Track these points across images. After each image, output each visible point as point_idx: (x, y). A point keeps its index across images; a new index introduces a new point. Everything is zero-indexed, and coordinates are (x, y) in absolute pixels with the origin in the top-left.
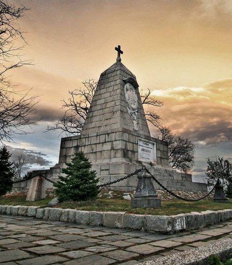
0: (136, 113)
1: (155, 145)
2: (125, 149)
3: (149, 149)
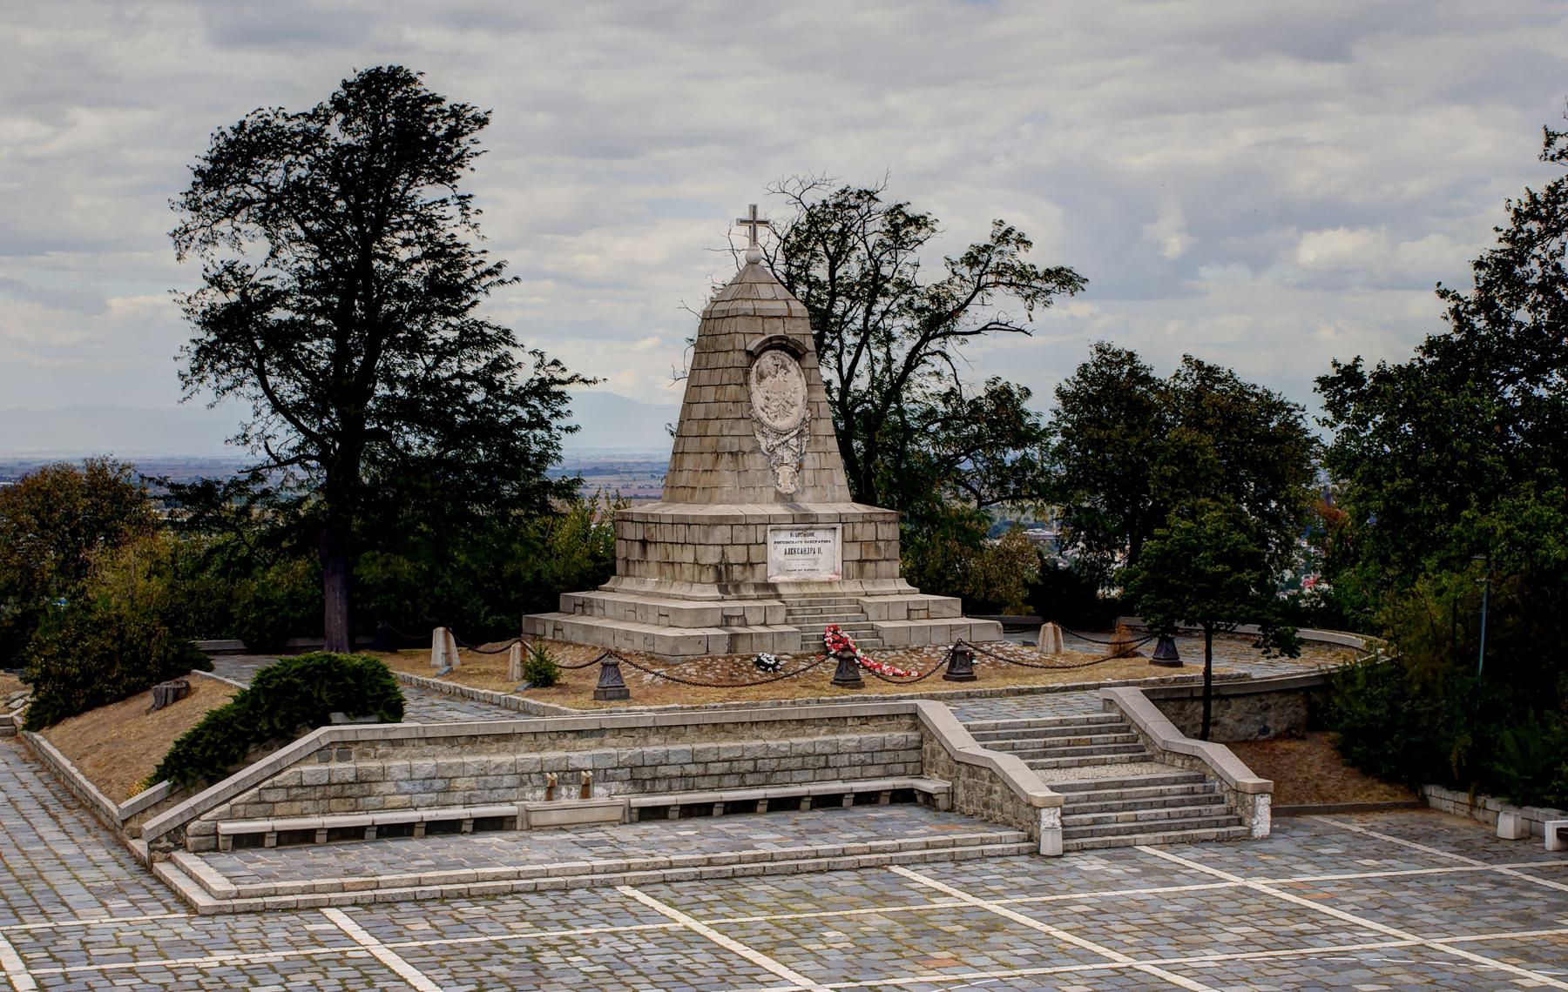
0: (794, 442)
1: (839, 532)
2: (721, 563)
3: (816, 546)
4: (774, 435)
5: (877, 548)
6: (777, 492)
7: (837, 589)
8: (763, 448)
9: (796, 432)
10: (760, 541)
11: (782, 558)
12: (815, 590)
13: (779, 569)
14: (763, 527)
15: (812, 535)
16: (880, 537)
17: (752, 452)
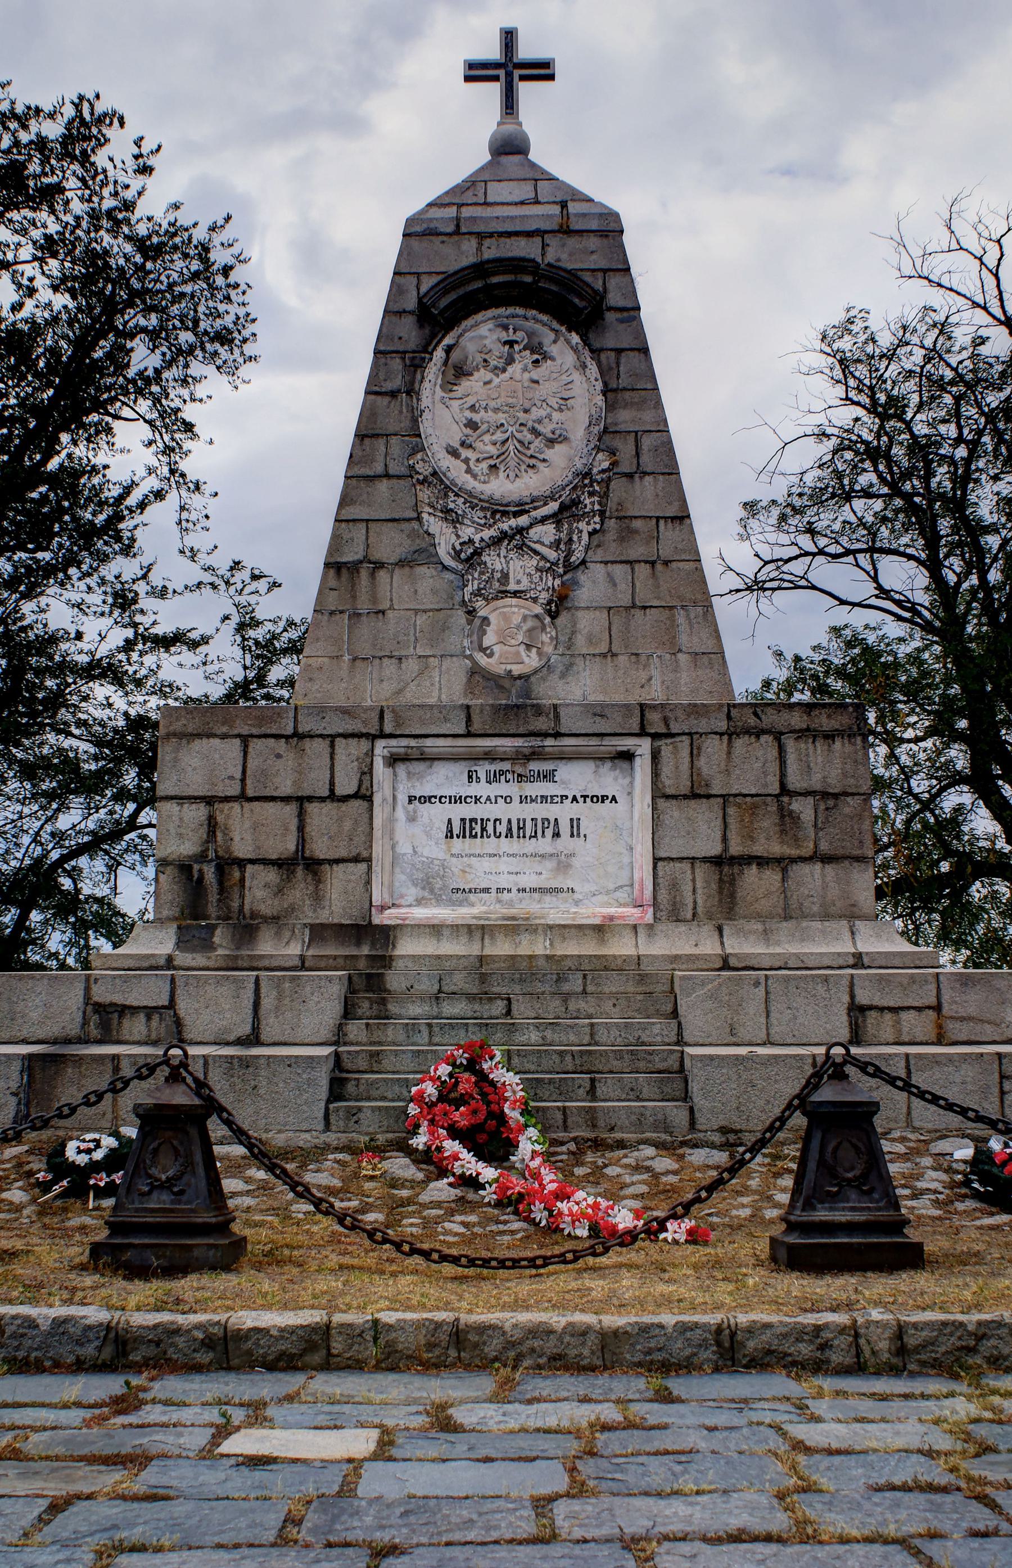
0: (547, 532)
1: (642, 766)
2: (202, 857)
3: (564, 812)
4: (477, 515)
5: (787, 820)
6: (476, 672)
7: (622, 947)
8: (443, 552)
9: (553, 506)
10: (346, 785)
11: (434, 849)
12: (540, 947)
13: (427, 884)
14: (357, 748)
15: (549, 776)
16: (795, 782)
17: (401, 563)
